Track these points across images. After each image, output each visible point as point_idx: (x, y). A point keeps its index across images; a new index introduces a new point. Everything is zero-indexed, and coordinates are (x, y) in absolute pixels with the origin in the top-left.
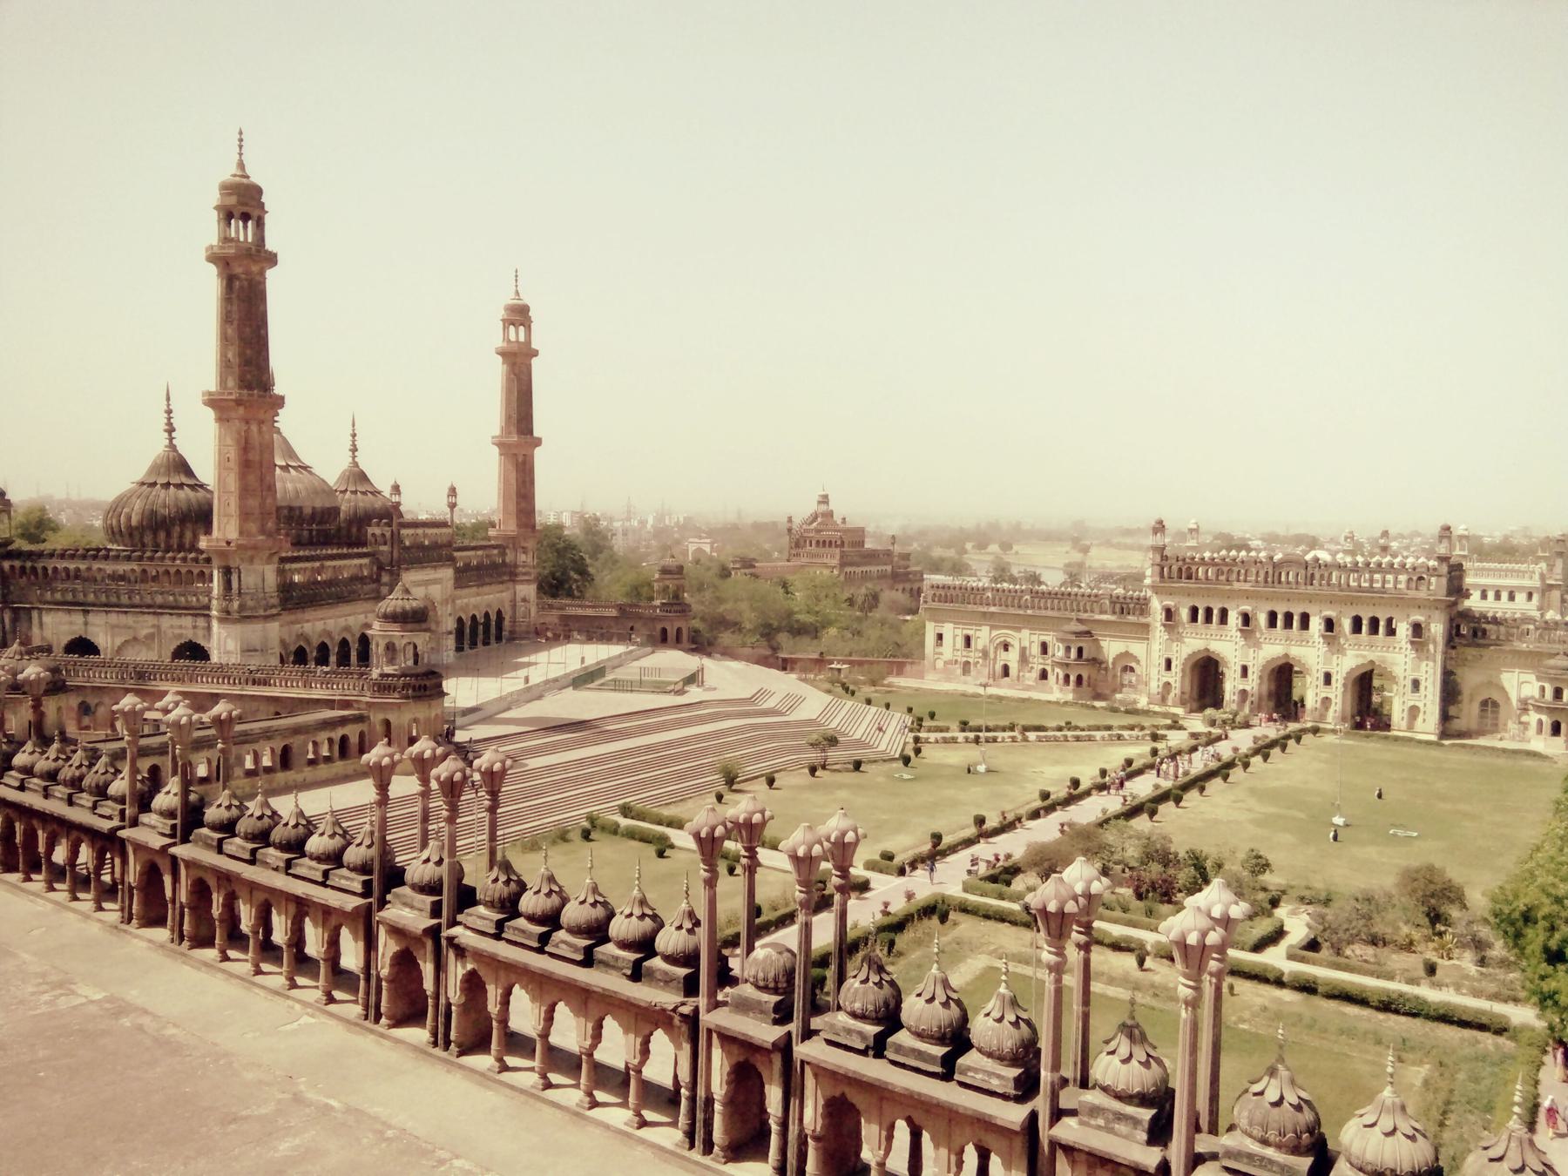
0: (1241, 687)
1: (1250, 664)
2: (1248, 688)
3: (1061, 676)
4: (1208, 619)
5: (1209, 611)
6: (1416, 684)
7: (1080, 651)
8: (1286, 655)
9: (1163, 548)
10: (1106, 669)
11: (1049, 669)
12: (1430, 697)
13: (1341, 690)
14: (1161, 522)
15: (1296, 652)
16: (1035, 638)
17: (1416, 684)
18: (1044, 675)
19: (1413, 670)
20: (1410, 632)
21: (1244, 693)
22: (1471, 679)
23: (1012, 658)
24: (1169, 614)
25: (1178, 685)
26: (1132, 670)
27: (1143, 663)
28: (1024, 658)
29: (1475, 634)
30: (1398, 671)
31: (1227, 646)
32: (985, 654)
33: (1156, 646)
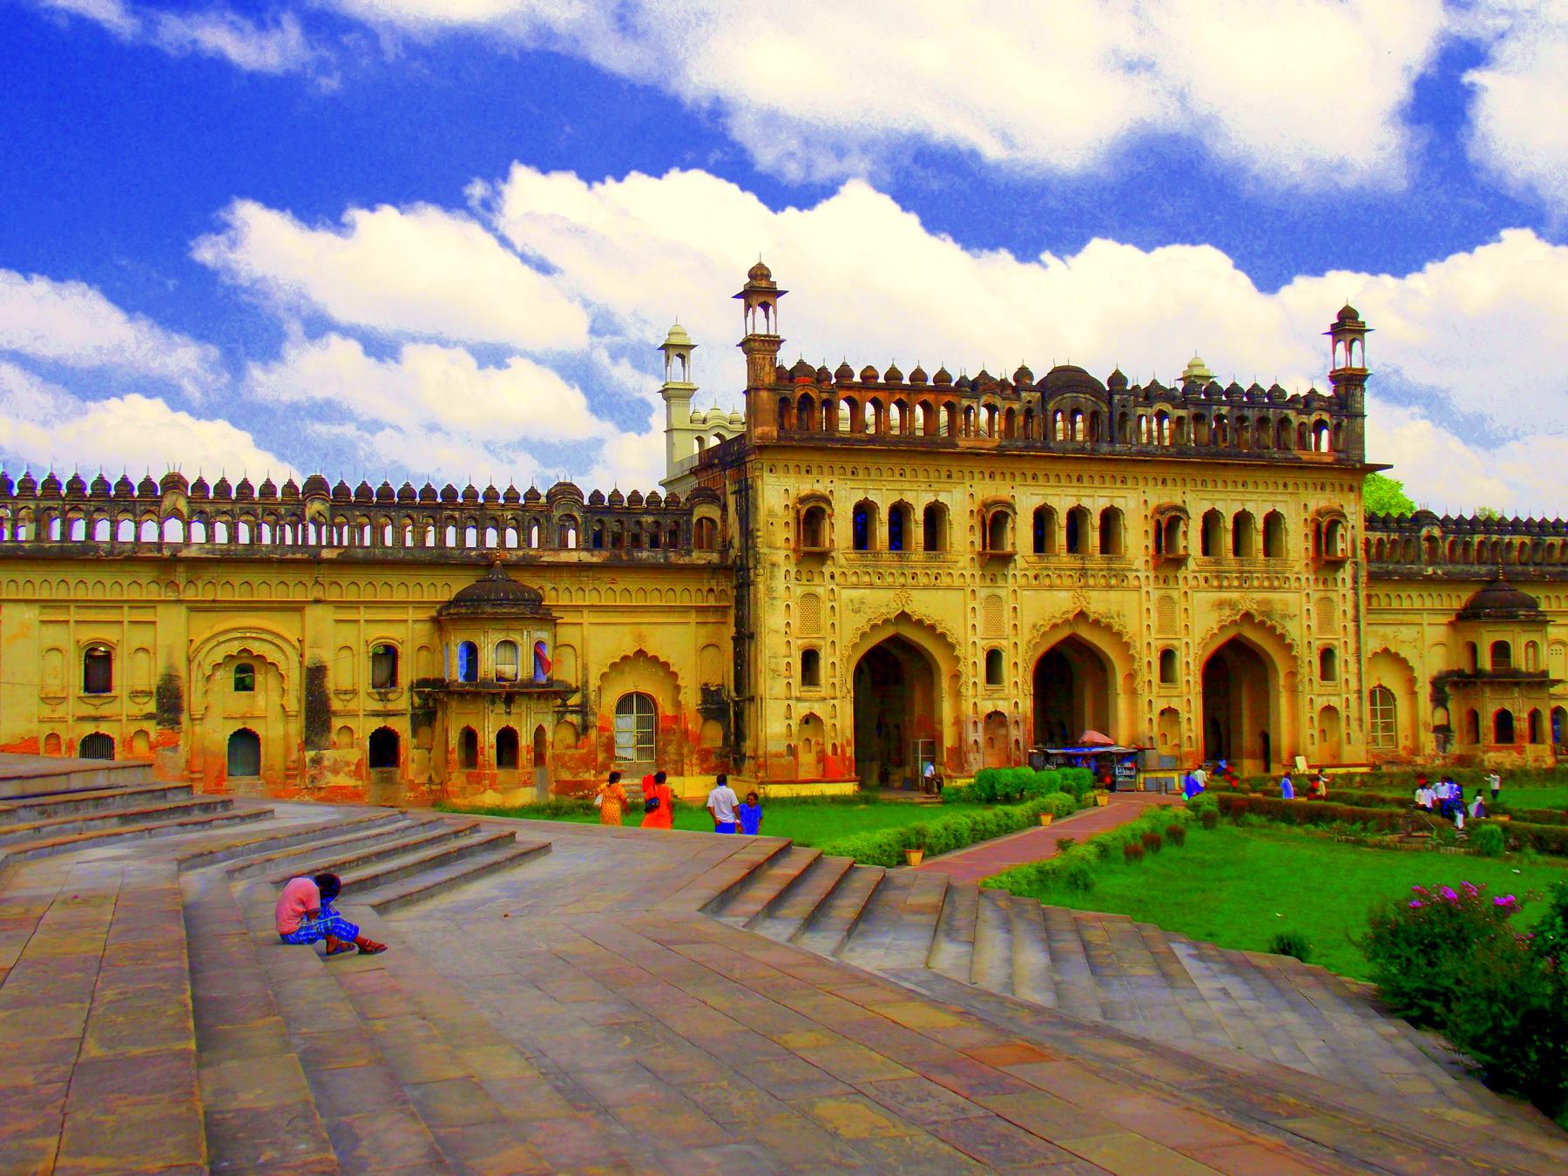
0: (988, 707)
1: (1005, 645)
2: (1003, 707)
3: (488, 739)
4: (898, 539)
5: (899, 513)
8: (1081, 615)
9: (774, 342)
10: (583, 709)
11: (402, 726)
12: (1353, 685)
14: (759, 273)
15: (1099, 602)
16: (348, 634)
18: (384, 748)
19: (1321, 629)
21: (995, 718)
23: (274, 713)
28: (317, 713)
32: (170, 702)
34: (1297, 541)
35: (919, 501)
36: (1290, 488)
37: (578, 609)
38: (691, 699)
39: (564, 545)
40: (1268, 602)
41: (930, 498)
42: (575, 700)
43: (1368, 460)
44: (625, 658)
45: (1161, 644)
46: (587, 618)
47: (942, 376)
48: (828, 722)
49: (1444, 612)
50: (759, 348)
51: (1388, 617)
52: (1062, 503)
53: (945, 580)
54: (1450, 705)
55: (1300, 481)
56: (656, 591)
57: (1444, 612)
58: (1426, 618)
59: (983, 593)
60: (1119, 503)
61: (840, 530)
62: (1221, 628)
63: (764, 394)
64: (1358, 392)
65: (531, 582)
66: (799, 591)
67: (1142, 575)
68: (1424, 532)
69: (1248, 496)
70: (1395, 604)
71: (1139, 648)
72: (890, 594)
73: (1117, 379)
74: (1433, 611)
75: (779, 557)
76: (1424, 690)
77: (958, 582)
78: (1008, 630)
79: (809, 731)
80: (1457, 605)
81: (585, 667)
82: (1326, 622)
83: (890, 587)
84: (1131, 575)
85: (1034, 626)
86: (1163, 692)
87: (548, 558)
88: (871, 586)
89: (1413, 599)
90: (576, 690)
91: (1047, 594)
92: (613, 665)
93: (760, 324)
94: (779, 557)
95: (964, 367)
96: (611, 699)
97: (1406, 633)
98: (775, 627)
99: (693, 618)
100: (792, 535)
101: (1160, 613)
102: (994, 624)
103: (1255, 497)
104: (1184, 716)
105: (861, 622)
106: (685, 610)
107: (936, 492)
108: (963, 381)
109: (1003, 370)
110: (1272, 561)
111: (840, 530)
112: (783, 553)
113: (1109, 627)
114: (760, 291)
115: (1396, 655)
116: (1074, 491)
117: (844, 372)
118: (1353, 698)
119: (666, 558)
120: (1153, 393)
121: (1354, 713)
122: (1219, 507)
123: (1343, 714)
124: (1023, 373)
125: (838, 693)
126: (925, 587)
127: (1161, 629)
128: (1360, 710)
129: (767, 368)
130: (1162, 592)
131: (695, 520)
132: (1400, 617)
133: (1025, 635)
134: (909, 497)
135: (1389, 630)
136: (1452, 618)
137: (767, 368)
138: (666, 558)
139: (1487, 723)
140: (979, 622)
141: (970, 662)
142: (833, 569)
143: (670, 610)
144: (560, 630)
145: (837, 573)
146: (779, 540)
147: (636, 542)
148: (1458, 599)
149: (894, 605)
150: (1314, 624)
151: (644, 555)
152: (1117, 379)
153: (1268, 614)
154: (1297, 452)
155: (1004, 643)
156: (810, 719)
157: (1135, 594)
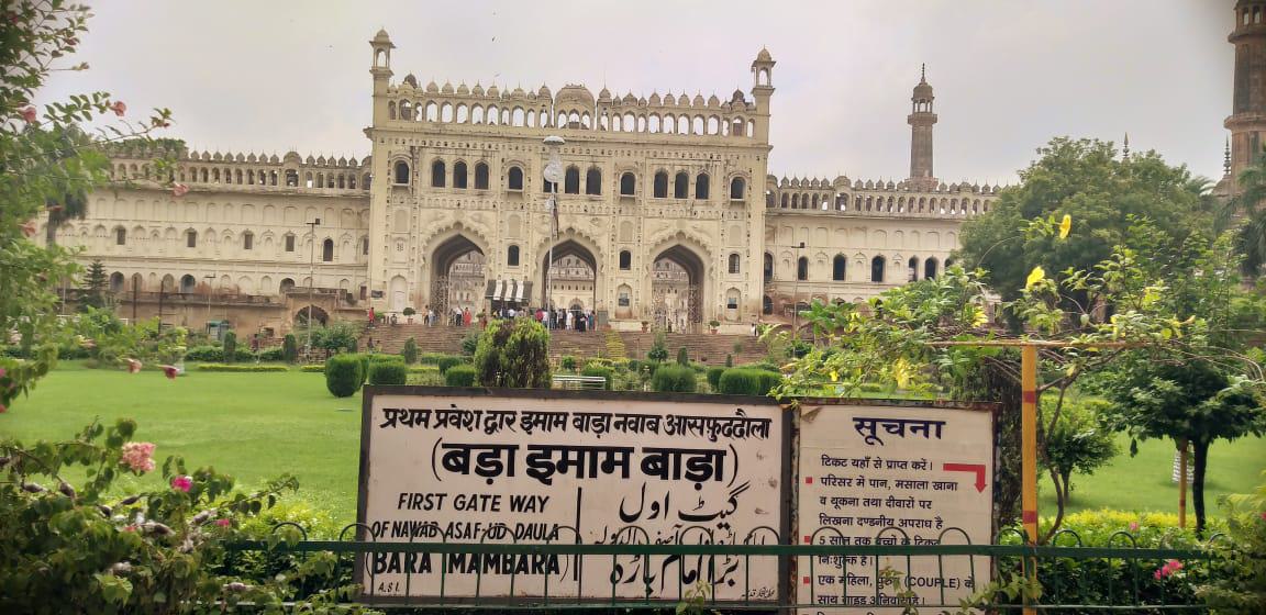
50: (380, 75)
73: (605, 93)
93: (382, 61)
95: (506, 85)
109: (531, 87)
124: (544, 93)
152: (605, 93)
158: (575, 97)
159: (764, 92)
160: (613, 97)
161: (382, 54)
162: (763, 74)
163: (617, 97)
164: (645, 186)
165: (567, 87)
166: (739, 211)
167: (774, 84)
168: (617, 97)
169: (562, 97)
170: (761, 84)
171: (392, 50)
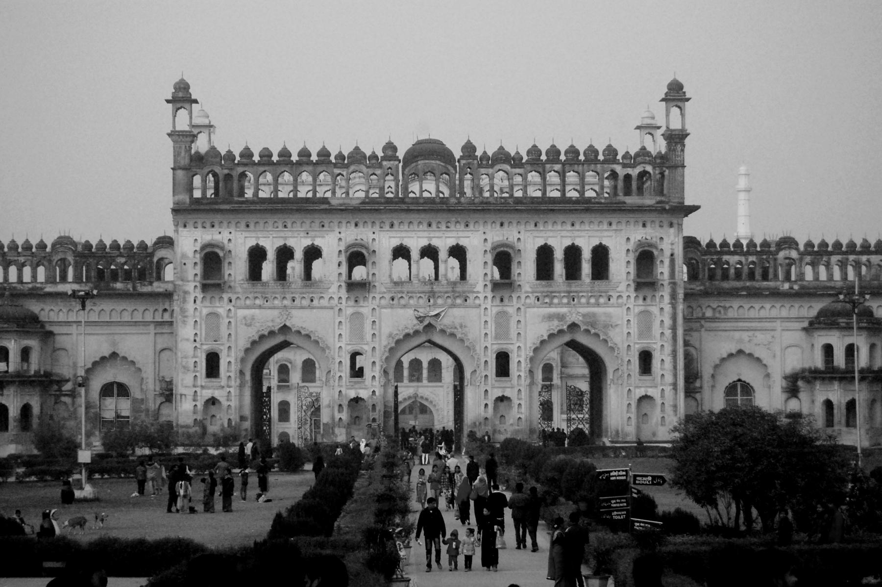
0: (352, 394)
2: (364, 394)
5: (285, 254)
6: (646, 358)
7: (25, 353)
12: (669, 378)
13: (525, 382)
17: (646, 358)
19: (641, 335)
20: (632, 269)
21: (357, 400)
22: (715, 346)
24: (212, 260)
25: (234, 403)
26: (123, 390)
27: (149, 373)
29: (712, 277)
30: (617, 337)
31: (327, 320)
33: (186, 331)
34: (621, 266)
35: (299, 244)
36: (614, 227)
37: (68, 323)
38: (152, 386)
39: (64, 279)
40: (594, 315)
41: (307, 242)
42: (68, 387)
43: (688, 202)
44: (103, 358)
45: (496, 348)
46: (73, 329)
47: (324, 154)
48: (225, 403)
49: (799, 319)
50: (182, 139)
51: (728, 325)
52: (415, 242)
53: (315, 302)
54: (802, 395)
55: (624, 221)
56: (124, 310)
57: (799, 319)
58: (778, 325)
59: (350, 311)
60: (463, 242)
61: (237, 269)
62: (551, 336)
63: (180, 173)
64: (679, 147)
65: (34, 307)
66: (205, 311)
67: (481, 296)
68: (782, 255)
69: (576, 234)
70: (753, 314)
71: (479, 349)
72: (276, 312)
73: (469, 149)
74: (788, 319)
75: (190, 287)
76: (778, 384)
77: (324, 302)
78: (368, 337)
79: (213, 410)
80: (814, 313)
81: (75, 365)
82: (645, 329)
83: (274, 308)
84: (472, 296)
85: (390, 335)
86: (497, 384)
87: (49, 289)
88: (260, 307)
89: (767, 309)
90: (68, 381)
91: (401, 311)
92: (95, 364)
93: (183, 122)
94: (190, 287)
96: (96, 384)
97: (760, 337)
98: (186, 337)
99: (152, 327)
100: (199, 270)
101: (498, 325)
102: (357, 332)
103: (583, 234)
104: (516, 402)
105: (253, 333)
106: (146, 324)
107: (313, 238)
108: (340, 156)
109: (373, 146)
110: (597, 282)
111: (237, 269)
112: (192, 285)
113: (453, 335)
114: (182, 97)
115: (750, 355)
116: (426, 234)
117: (247, 154)
118: (668, 389)
119: (134, 288)
120: (502, 157)
121: (669, 402)
122: (550, 242)
123: (659, 401)
124: (390, 148)
125: (233, 383)
126: (302, 308)
127: (497, 337)
128: (675, 399)
129: (183, 154)
130: (500, 309)
131: (155, 259)
132: (753, 324)
133: (384, 342)
134: (291, 243)
135: (745, 335)
136: (806, 324)
137: (183, 154)
138: (134, 288)
139: (819, 410)
140: (345, 330)
141: (338, 361)
142: (230, 295)
143: (136, 323)
144: (58, 338)
145: (233, 298)
146: (191, 277)
147: (115, 276)
148: (813, 308)
149: (278, 320)
150: (634, 329)
151: (119, 285)
152: (469, 149)
153: (593, 324)
154: (621, 197)
155: (366, 347)
156: (213, 401)
157: (473, 312)
158: (429, 154)
159: (676, 138)
160: (479, 153)
161: (183, 113)
162: (675, 111)
163: (485, 153)
164: (525, 269)
165: (419, 143)
166: (649, 294)
167: (689, 128)
168: (485, 153)
169: (413, 156)
170: (672, 127)
171: (194, 105)
